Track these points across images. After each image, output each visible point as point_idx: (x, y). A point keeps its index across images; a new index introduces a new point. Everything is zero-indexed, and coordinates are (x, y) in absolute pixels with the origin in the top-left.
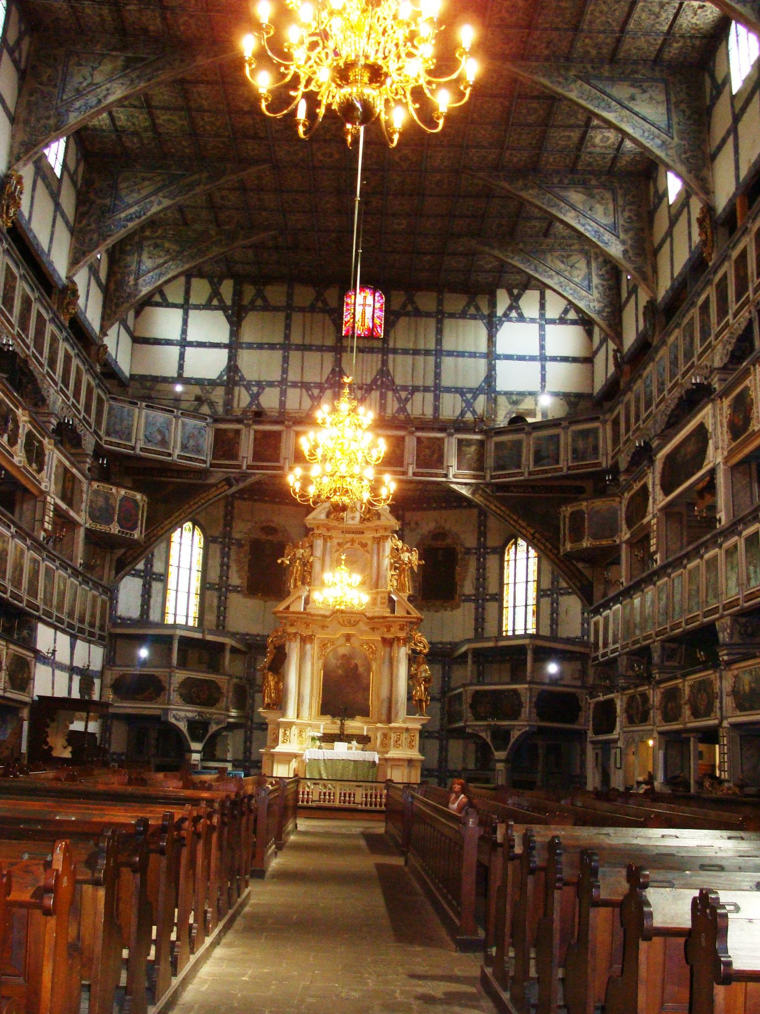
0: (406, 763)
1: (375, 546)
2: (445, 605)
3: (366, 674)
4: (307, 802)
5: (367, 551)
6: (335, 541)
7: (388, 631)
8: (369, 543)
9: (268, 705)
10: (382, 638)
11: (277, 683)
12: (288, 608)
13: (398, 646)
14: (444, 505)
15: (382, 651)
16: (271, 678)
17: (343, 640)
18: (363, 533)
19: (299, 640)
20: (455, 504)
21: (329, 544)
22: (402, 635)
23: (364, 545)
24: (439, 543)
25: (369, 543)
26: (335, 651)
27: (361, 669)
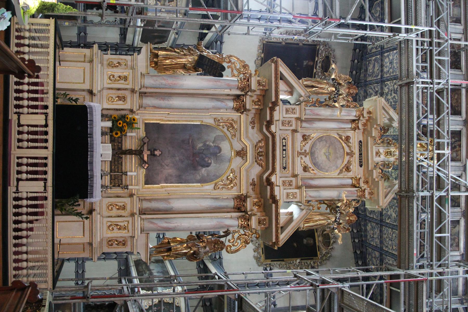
0: (86, 239)
1: (349, 182)
2: (260, 251)
3: (198, 177)
4: (17, 106)
5: (341, 171)
6: (350, 133)
7: (255, 204)
8: (351, 174)
9: (157, 56)
10: (246, 197)
11: (184, 67)
12: (282, 78)
13: (238, 218)
14: (357, 241)
15: (227, 196)
16: (190, 59)
17: (238, 147)
18: (361, 166)
19: (238, 92)
20: (358, 252)
21: (349, 126)
22: (254, 222)
23: (348, 169)
24: (319, 239)
25: (351, 174)
26: (225, 137)
27: (204, 171)
